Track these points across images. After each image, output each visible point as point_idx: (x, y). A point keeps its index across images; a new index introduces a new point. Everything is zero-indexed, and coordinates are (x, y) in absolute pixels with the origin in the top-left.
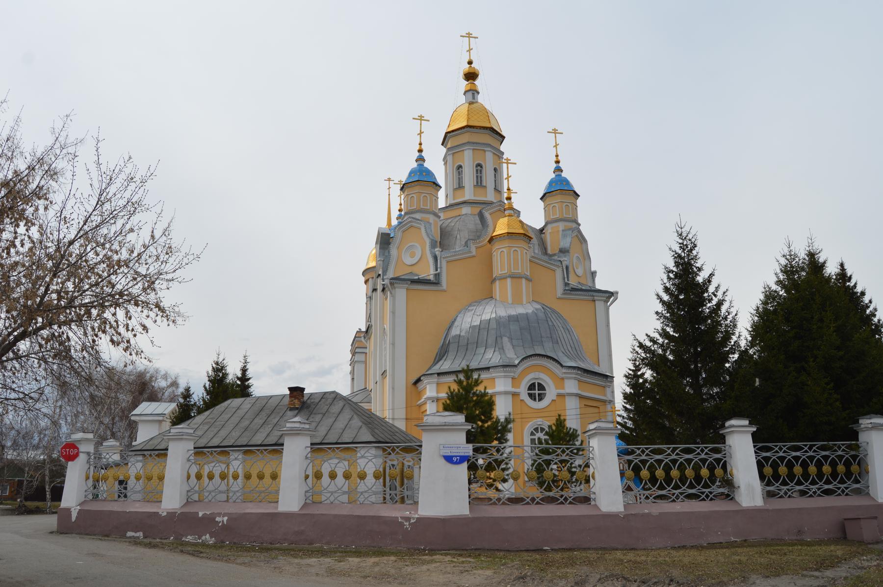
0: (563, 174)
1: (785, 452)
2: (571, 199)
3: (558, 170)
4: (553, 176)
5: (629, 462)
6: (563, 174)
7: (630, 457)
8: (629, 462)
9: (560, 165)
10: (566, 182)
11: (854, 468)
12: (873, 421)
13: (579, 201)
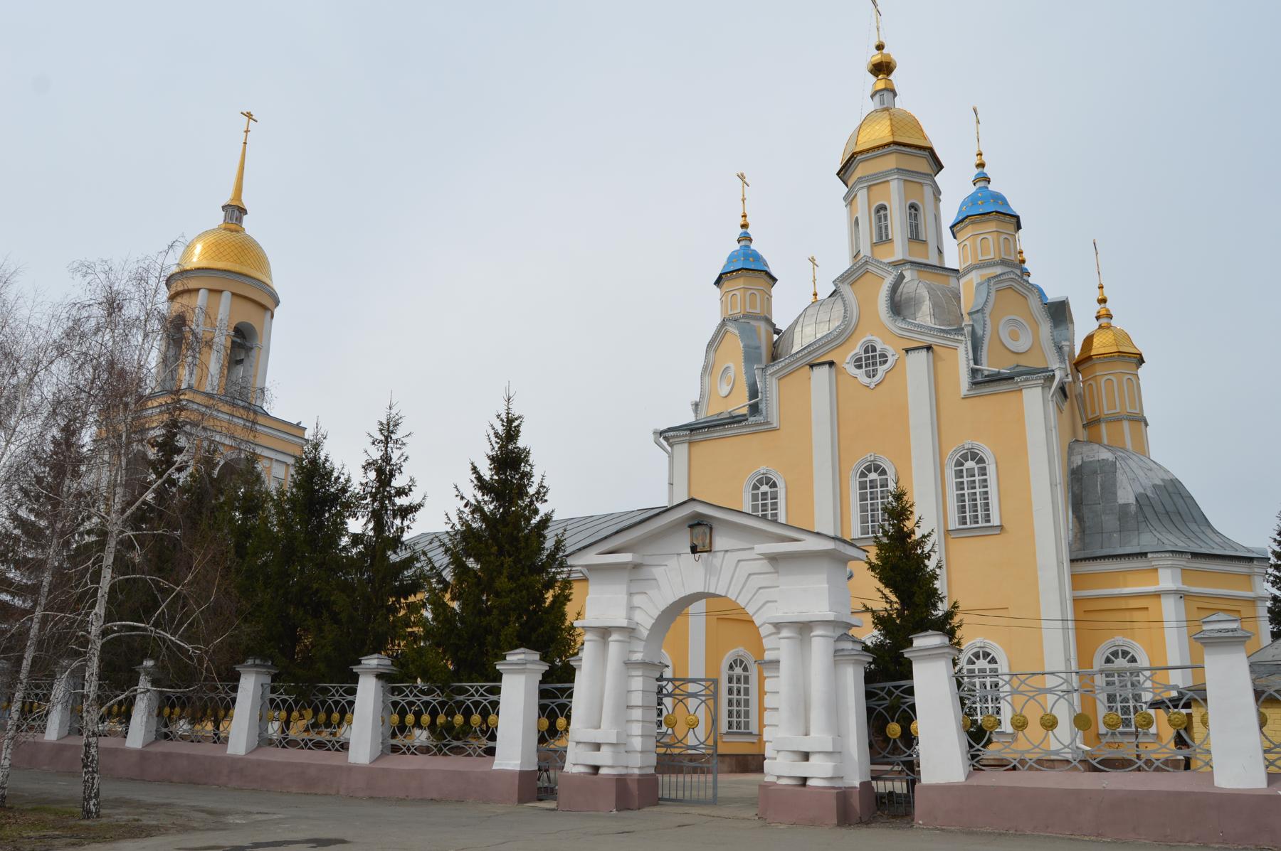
0: (753, 246)
1: (482, 695)
2: (761, 282)
3: (745, 238)
4: (737, 247)
5: (395, 704)
6: (753, 246)
7: (397, 698)
8: (395, 704)
9: (749, 231)
10: (757, 257)
11: (561, 722)
12: (96, 660)
13: (775, 290)
